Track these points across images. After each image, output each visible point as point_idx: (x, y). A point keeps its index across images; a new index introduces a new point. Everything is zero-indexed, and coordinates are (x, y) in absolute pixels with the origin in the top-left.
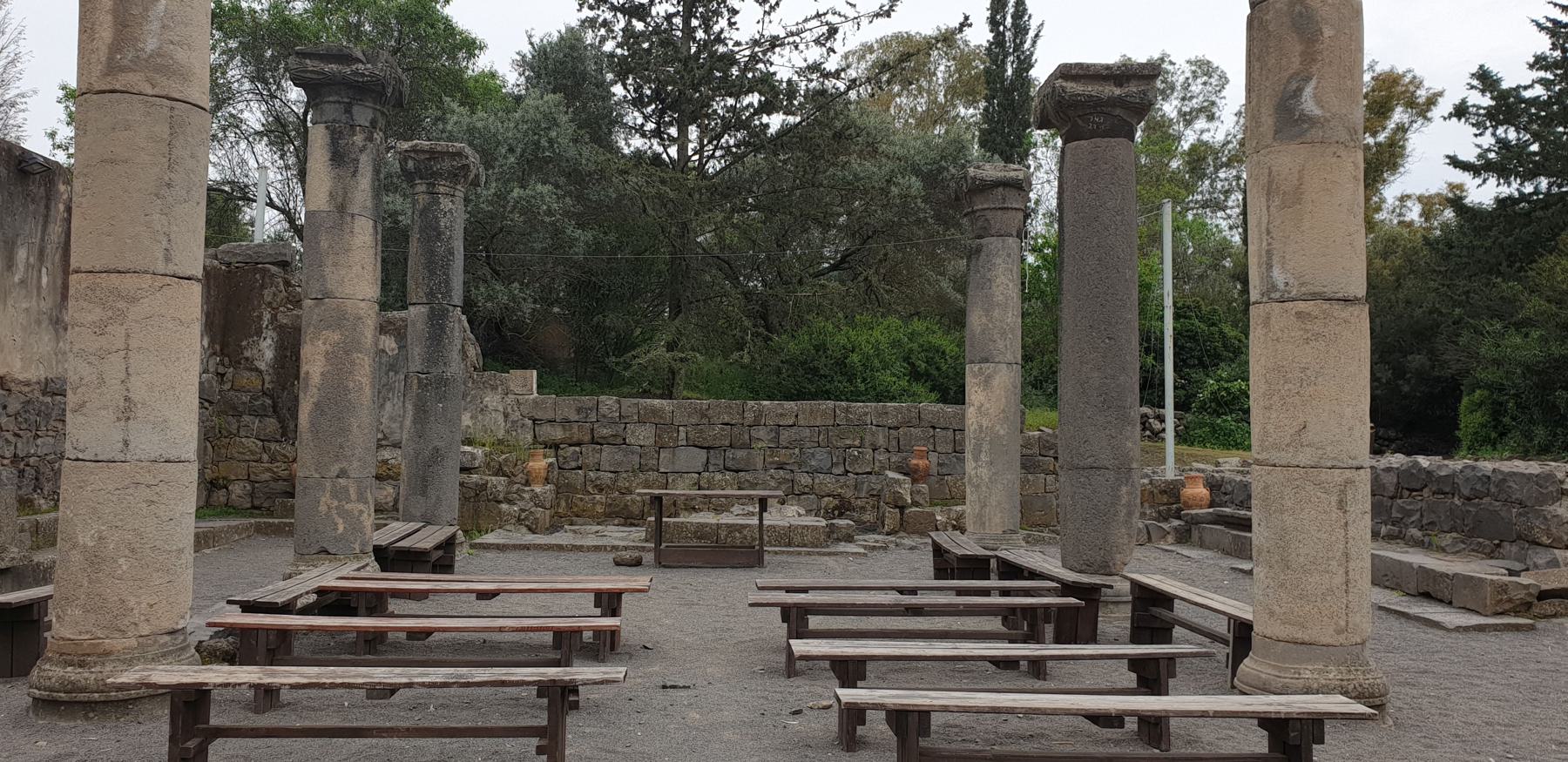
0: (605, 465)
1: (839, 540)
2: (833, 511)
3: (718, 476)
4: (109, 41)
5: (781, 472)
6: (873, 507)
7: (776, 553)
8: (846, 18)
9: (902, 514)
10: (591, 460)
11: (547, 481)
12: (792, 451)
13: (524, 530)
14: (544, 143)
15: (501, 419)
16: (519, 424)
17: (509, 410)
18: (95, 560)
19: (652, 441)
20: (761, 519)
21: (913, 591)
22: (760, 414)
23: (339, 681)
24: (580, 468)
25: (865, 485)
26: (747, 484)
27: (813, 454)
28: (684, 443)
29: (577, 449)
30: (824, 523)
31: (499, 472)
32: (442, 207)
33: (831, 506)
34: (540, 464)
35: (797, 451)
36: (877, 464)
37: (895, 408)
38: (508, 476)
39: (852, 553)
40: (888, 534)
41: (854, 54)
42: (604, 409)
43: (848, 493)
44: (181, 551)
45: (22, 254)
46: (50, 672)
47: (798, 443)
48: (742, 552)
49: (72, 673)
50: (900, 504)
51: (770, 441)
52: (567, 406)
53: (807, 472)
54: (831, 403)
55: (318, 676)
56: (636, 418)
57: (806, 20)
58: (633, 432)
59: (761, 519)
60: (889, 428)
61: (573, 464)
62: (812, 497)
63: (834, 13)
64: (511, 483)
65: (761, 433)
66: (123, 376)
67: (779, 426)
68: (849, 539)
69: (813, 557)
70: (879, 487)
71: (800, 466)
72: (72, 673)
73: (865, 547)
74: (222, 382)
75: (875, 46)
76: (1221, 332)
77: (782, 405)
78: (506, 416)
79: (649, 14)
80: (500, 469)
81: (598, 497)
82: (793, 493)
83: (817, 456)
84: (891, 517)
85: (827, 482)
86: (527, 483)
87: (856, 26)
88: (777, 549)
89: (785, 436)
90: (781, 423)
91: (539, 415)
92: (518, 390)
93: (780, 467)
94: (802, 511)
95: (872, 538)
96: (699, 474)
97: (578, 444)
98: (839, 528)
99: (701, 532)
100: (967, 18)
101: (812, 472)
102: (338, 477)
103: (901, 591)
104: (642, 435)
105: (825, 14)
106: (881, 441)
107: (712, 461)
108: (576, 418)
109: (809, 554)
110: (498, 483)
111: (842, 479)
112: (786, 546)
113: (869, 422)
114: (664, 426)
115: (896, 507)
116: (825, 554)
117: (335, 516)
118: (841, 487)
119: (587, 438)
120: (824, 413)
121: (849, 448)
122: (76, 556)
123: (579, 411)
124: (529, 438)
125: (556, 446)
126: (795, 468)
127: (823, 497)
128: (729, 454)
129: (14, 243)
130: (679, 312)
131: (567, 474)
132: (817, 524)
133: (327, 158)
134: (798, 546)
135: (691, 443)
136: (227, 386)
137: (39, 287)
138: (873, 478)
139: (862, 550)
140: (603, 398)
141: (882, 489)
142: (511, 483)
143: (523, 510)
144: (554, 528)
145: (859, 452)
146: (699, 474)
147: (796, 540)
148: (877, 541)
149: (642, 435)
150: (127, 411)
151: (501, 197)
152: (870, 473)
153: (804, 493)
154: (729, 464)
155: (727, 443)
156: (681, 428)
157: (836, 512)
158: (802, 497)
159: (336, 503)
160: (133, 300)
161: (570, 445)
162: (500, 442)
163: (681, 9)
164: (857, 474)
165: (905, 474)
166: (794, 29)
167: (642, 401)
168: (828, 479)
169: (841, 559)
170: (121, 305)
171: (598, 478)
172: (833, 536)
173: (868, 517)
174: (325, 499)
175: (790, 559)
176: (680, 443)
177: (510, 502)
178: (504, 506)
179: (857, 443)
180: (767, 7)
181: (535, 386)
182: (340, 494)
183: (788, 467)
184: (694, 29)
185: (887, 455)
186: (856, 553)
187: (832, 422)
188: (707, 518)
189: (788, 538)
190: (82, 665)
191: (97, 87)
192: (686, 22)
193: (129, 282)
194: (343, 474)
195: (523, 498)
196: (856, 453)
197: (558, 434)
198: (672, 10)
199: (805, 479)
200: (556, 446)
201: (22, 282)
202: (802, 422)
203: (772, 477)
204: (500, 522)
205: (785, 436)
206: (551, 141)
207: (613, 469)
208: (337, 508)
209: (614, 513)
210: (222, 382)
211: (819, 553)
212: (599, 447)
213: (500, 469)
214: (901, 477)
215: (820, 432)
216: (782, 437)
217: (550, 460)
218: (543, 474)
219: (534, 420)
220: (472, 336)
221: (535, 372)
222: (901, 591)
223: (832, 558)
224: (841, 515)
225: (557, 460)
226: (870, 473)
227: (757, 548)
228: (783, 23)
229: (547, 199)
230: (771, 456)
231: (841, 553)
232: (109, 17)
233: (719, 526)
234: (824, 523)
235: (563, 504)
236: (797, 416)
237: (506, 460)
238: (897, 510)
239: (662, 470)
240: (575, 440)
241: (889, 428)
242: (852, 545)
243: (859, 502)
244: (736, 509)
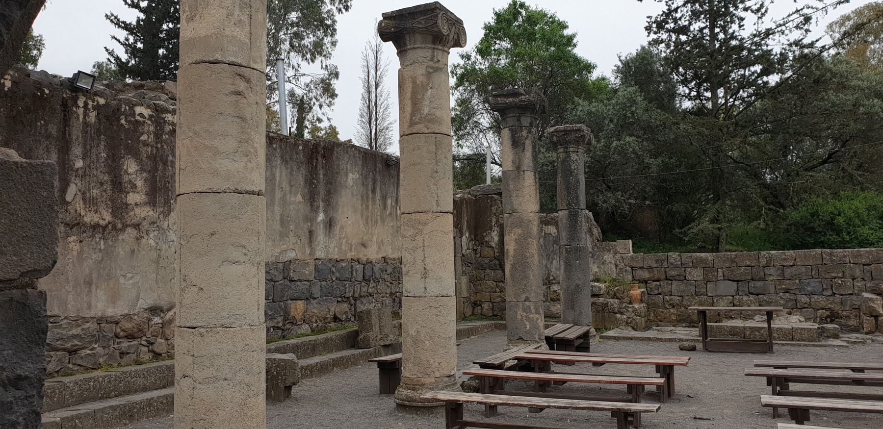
0: (675, 292)
1: (828, 337)
2: (826, 319)
3: (745, 298)
4: (410, 112)
5: (787, 295)
6: (856, 316)
7: (783, 345)
8: (817, 9)
9: (876, 320)
10: (666, 290)
11: (641, 301)
12: (794, 282)
13: (630, 329)
14: (629, 114)
15: (614, 267)
16: (624, 270)
17: (618, 262)
18: (416, 342)
19: (702, 277)
20: (769, 324)
21: (861, 370)
22: (770, 259)
23: (516, 403)
24: (660, 294)
25: (849, 302)
26: (764, 303)
27: (808, 283)
28: (722, 278)
29: (658, 283)
30: (816, 326)
31: (615, 296)
32: (572, 158)
33: (825, 316)
34: (636, 292)
35: (797, 281)
36: (856, 288)
37: (867, 251)
38: (620, 299)
39: (837, 346)
40: (867, 333)
41: (836, 23)
42: (671, 260)
43: (837, 308)
44: (450, 338)
45: (389, 202)
46: (402, 392)
48: (758, 344)
49: (410, 393)
50: (874, 314)
51: (778, 276)
52: (650, 259)
53: (806, 295)
54: (818, 251)
55: (508, 399)
56: (691, 264)
57: (789, 16)
58: (690, 273)
59: (769, 324)
60: (864, 265)
61: (656, 292)
62: (810, 310)
63: (808, 8)
64: (622, 303)
65: (772, 271)
66: (423, 258)
67: (784, 266)
68: (836, 337)
69: (809, 348)
70: (859, 303)
72: (410, 393)
73: (848, 342)
74: (476, 254)
75: (852, 15)
77: (784, 253)
78: (616, 266)
79: (689, 30)
80: (615, 295)
81: (672, 310)
82: (794, 308)
83: (812, 284)
84: (868, 322)
85: (821, 300)
86: (631, 303)
87: (824, 13)
88: (784, 342)
89: (788, 272)
90: (785, 264)
91: (634, 265)
92: (622, 251)
93: (786, 291)
94: (802, 319)
95: (854, 336)
96: (733, 296)
97: (658, 281)
98: (828, 330)
99: (733, 331)
101: (810, 294)
102: (525, 301)
103: (854, 370)
104: (696, 274)
105: (802, 9)
106: (858, 273)
107: (741, 289)
108: (656, 265)
109: (805, 345)
110: (614, 303)
111: (831, 299)
112: (790, 340)
113: (848, 261)
114: (708, 269)
115: (872, 316)
116: (818, 346)
117: (525, 321)
118: (831, 304)
119: (663, 277)
120: (814, 257)
121: (835, 278)
122: (409, 340)
123: (657, 261)
124: (630, 277)
125: (645, 282)
126: (797, 292)
127: (818, 310)
128: (752, 284)
129: (386, 197)
130: (719, 199)
131: (653, 298)
132: (811, 327)
133: (510, 144)
134: (799, 341)
135: (727, 278)
136: (478, 256)
137: (397, 216)
138: (854, 297)
139: (845, 344)
140: (670, 254)
141: (861, 304)
142: (622, 303)
143: (629, 318)
144: (647, 328)
145: (842, 281)
146: (733, 296)
147: (797, 336)
148: (857, 338)
149: (696, 274)
150: (425, 275)
151: (607, 146)
152: (852, 294)
153: (804, 308)
154: (752, 290)
155: (750, 278)
156: (719, 270)
157: (829, 320)
158: (804, 310)
159: (525, 314)
160: (425, 225)
161: (654, 281)
162: (614, 280)
163: (708, 24)
164: (842, 295)
165: (878, 295)
166: (782, 22)
167: (694, 254)
168: (820, 298)
169: (828, 349)
170: (421, 227)
171: (671, 300)
172: (822, 334)
173: (853, 322)
174: (520, 312)
175: (793, 349)
176: (719, 278)
177: (621, 313)
178: (618, 316)
179: (840, 275)
180: (760, 15)
181: (631, 249)
182: (527, 310)
183: (792, 292)
184: (717, 34)
185: (863, 282)
186: (840, 346)
187: (820, 263)
188: (738, 323)
189: (791, 336)
190: (414, 389)
191: (407, 133)
192: (712, 30)
193: (423, 217)
194: (527, 299)
195: (629, 311)
196: (840, 282)
197: (646, 275)
198: (703, 25)
199: (804, 299)
200: (645, 282)
201: (390, 214)
202: (799, 263)
203: (781, 298)
204: (617, 324)
205: (788, 272)
206: (633, 113)
207: (679, 295)
208: (526, 317)
209: (683, 320)
210: (476, 254)
211: (813, 345)
212: (670, 282)
213: (615, 295)
214: (874, 297)
215: (812, 269)
216: (786, 273)
217: (643, 290)
218: (639, 297)
219: (632, 268)
220: (595, 223)
221: (630, 241)
222: (854, 370)
223: (823, 348)
224: (832, 322)
225: (647, 290)
226: (852, 294)
227: (768, 341)
228: (774, 20)
229: (633, 145)
230: (780, 285)
231: (830, 345)
232: (410, 102)
233: (745, 328)
234: (816, 326)
235: (652, 314)
236: (795, 259)
237: (618, 290)
238: (873, 318)
239: (709, 295)
240: (656, 278)
241: (864, 265)
242: (838, 341)
243: (845, 313)
244: (757, 318)
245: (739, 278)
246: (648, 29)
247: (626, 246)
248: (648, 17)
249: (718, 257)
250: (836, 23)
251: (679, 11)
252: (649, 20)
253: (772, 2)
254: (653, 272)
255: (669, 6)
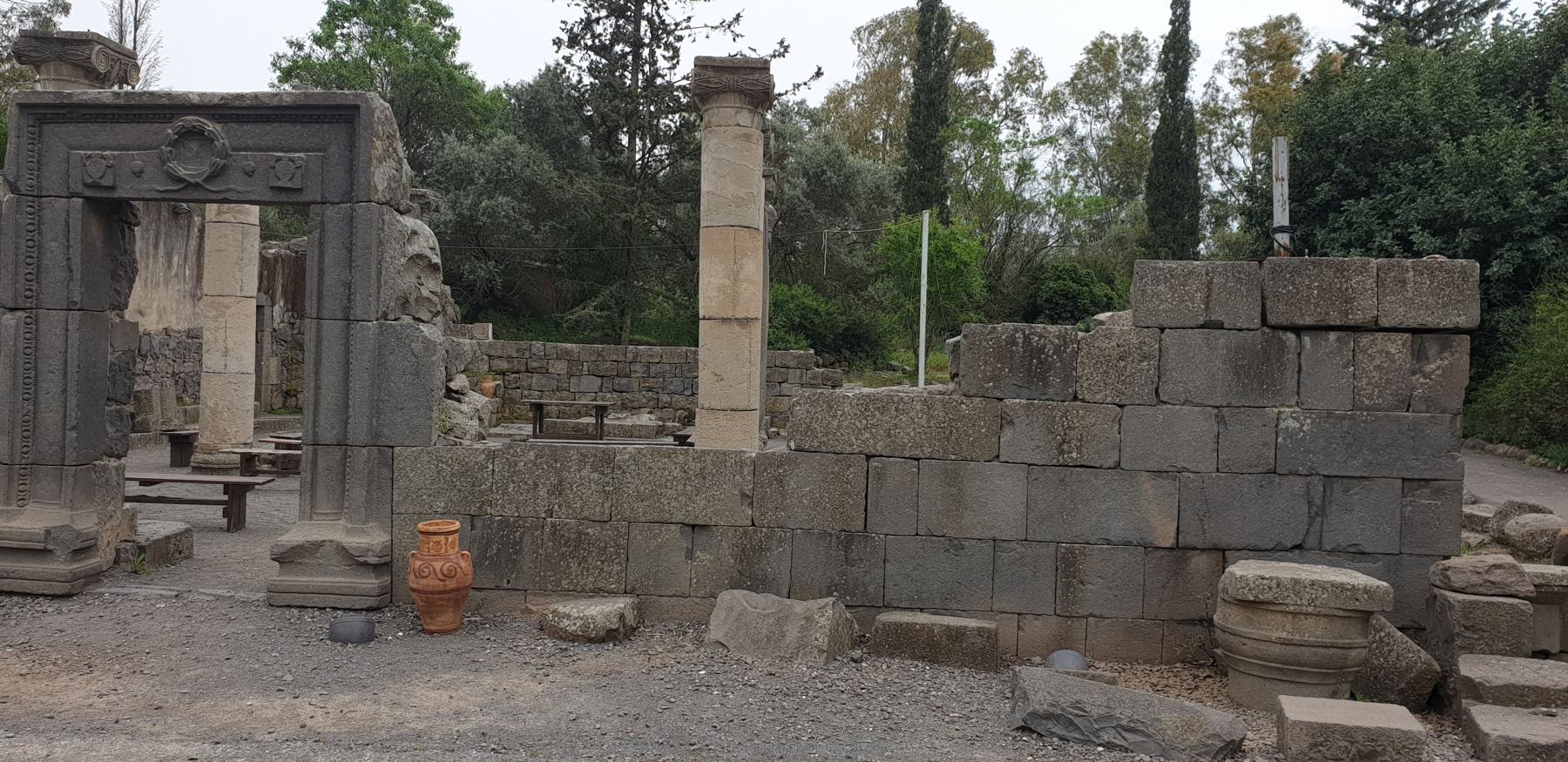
0: (534, 386)
3: (609, 395)
14: (503, 169)
18: (214, 413)
19: (565, 371)
22: (636, 355)
41: (865, 30)
42: (534, 350)
45: (175, 259)
46: (198, 457)
47: (663, 374)
49: (207, 457)
52: (510, 348)
61: (514, 386)
65: (638, 367)
71: (663, 389)
72: (207, 457)
74: (293, 329)
76: (1091, 292)
91: (492, 353)
93: (650, 389)
100: (820, 69)
104: (559, 367)
107: (605, 385)
108: (516, 355)
114: (573, 361)
119: (523, 369)
120: (680, 355)
122: (207, 411)
123: (518, 351)
124: (486, 368)
126: (660, 391)
129: (172, 253)
136: (296, 331)
137: (185, 277)
140: (534, 342)
149: (559, 367)
150: (226, 353)
151: (476, 204)
154: (616, 387)
155: (615, 373)
160: (228, 307)
167: (559, 344)
170: (224, 309)
181: (490, 334)
190: (210, 454)
193: (227, 300)
197: (504, 365)
199: (665, 398)
200: (503, 373)
201: (176, 275)
202: (665, 361)
205: (653, 369)
206: (509, 168)
210: (293, 329)
218: (492, 391)
220: (452, 300)
221: (491, 325)
235: (507, 411)
245: (604, 374)
246: (558, 42)
247: (486, 331)
248: (563, 22)
249: (583, 349)
250: (865, 30)
251: (601, 22)
252: (563, 26)
253: (707, 37)
254: (513, 362)
255: (589, 14)
